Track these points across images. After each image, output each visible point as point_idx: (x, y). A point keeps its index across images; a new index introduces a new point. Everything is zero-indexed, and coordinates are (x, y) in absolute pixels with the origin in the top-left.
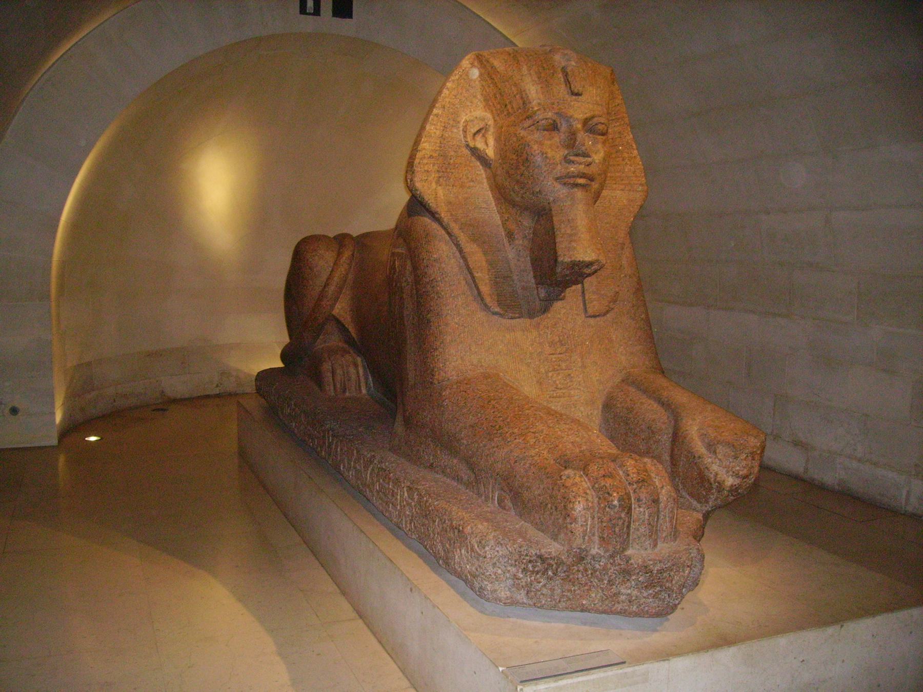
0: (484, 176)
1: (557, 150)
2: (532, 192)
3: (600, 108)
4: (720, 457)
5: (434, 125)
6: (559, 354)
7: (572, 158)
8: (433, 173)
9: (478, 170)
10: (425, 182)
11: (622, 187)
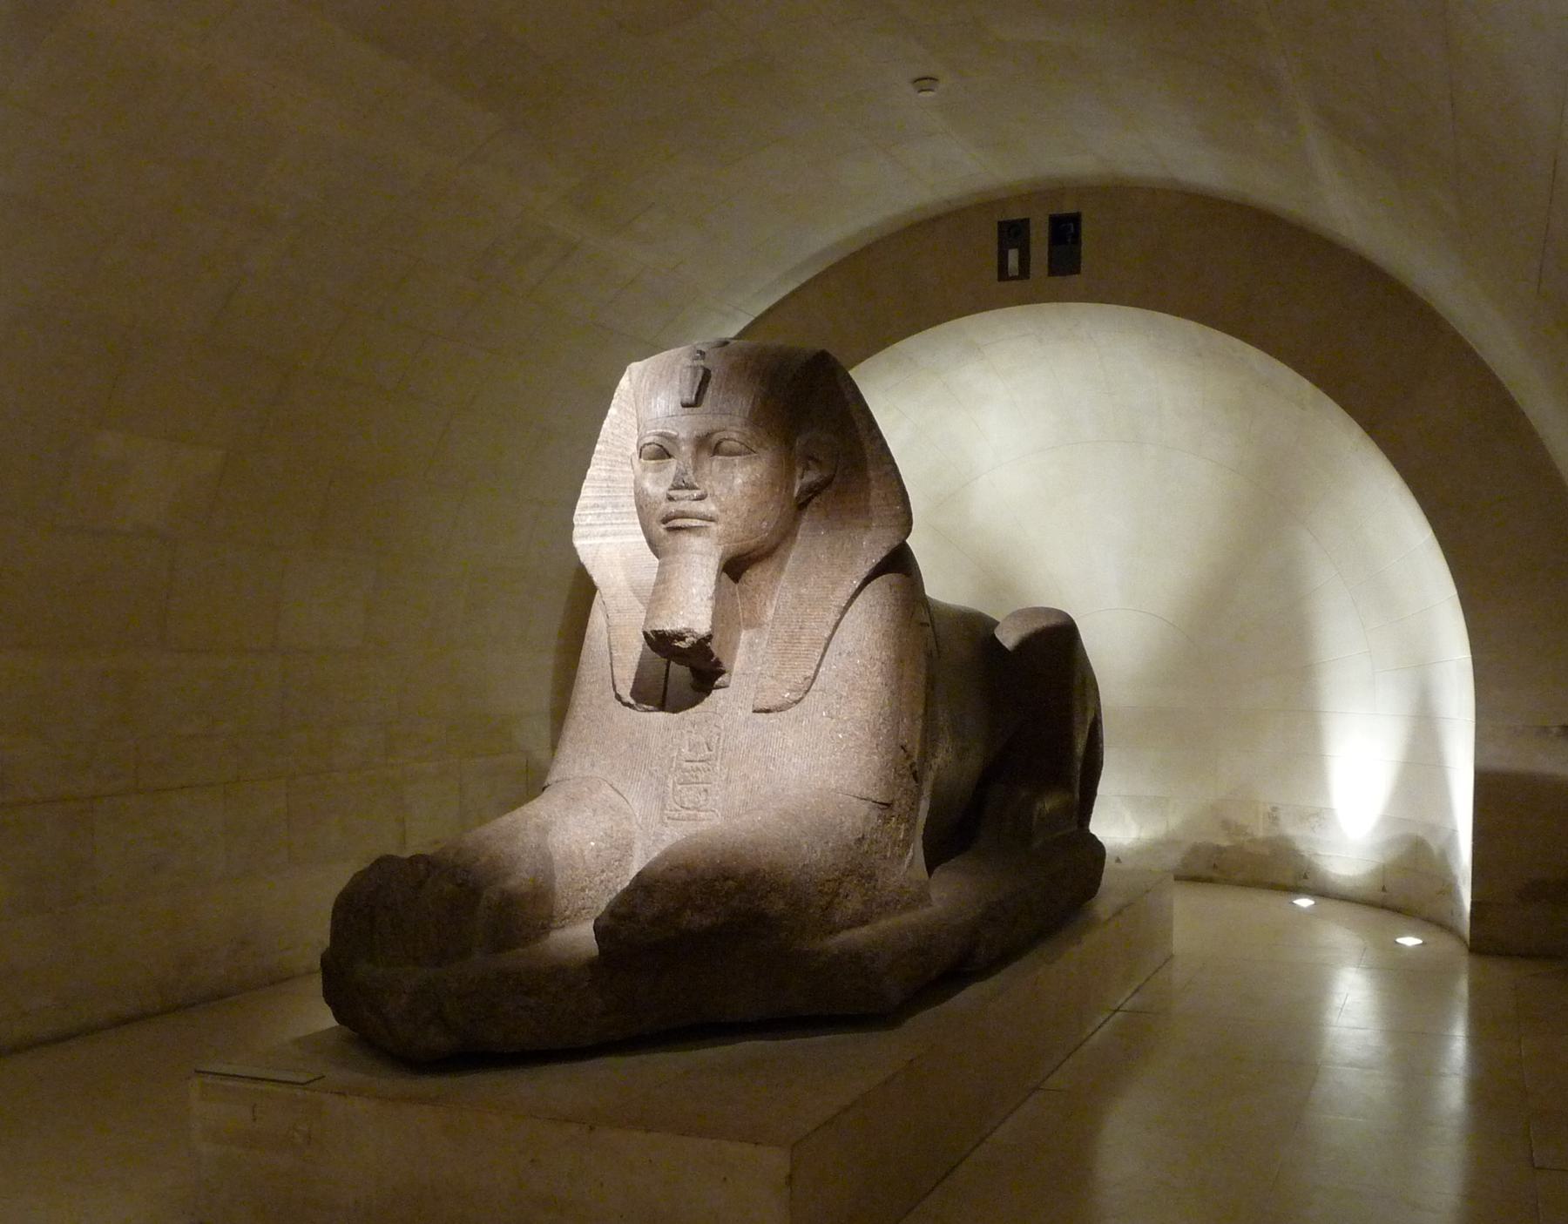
5: (597, 464)
7: (673, 493)
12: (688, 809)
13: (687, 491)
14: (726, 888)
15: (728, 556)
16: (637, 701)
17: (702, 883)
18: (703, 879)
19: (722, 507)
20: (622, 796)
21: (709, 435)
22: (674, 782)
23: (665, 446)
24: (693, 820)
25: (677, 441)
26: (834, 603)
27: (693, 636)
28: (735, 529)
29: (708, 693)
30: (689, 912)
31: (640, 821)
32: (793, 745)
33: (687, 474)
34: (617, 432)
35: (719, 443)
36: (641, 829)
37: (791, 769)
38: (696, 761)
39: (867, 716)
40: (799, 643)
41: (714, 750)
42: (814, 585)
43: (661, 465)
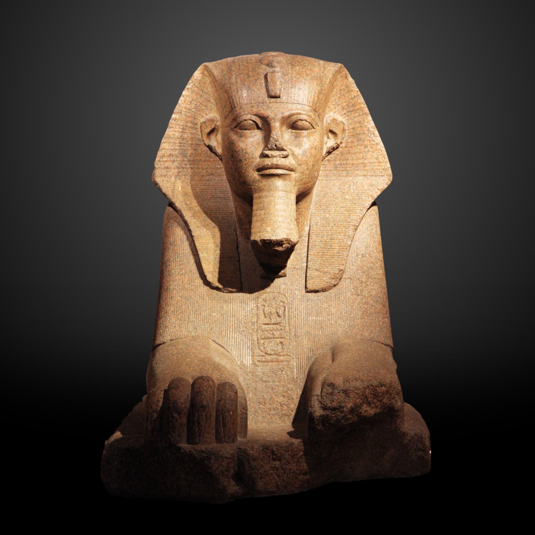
0: (223, 169)
1: (256, 146)
3: (299, 106)
5: (173, 128)
6: (273, 324)
7: (267, 152)
8: (173, 169)
9: (218, 165)
10: (165, 177)
11: (365, 173)
12: (270, 355)
13: (278, 152)
14: (382, 391)
15: (298, 193)
16: (225, 286)
17: (372, 388)
18: (372, 386)
19: (299, 163)
20: (224, 348)
21: (290, 116)
22: (257, 337)
23: (258, 122)
24: (276, 361)
25: (268, 120)
26: (351, 224)
27: (289, 244)
28: (305, 177)
29: (272, 281)
30: (365, 406)
31: (239, 363)
32: (336, 313)
33: (278, 141)
34: (188, 106)
35: (296, 121)
36: (241, 368)
37: (338, 327)
38: (270, 324)
39: (379, 294)
40: (332, 248)
41: (283, 316)
42: (335, 211)
43: (253, 134)
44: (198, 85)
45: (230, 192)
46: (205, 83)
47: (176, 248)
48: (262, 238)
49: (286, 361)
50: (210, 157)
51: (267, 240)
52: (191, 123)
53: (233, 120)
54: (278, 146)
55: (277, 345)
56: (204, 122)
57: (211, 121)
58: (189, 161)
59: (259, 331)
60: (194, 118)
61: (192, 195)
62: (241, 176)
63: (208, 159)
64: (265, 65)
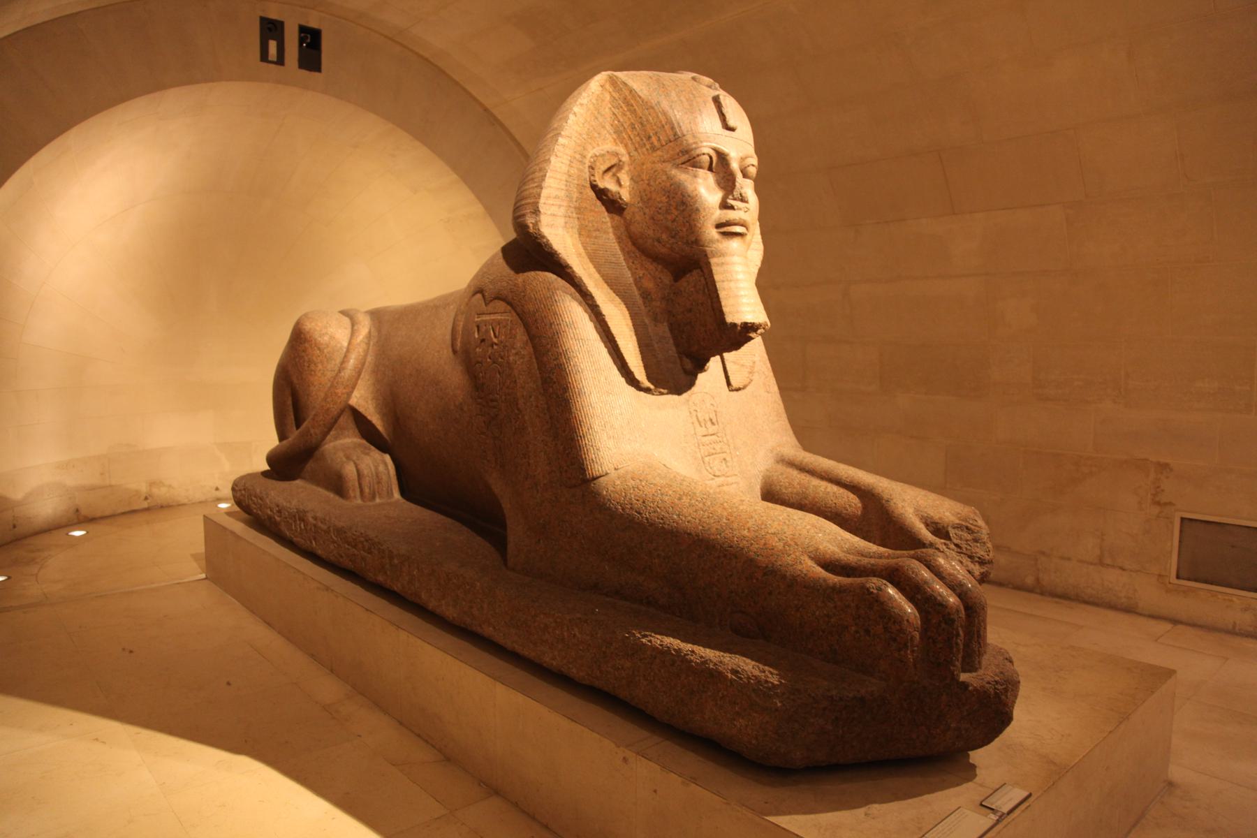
0: (609, 224)
2: (685, 241)
4: (956, 541)
12: (718, 476)
16: (656, 386)
25: (728, 158)
34: (579, 129)
35: (748, 166)
44: (595, 102)
45: (621, 256)
46: (603, 100)
47: (578, 332)
48: (743, 321)
49: (735, 483)
50: (595, 205)
51: (751, 323)
52: (580, 154)
53: (681, 151)
54: (743, 195)
55: (722, 462)
56: (602, 155)
57: (613, 155)
58: (575, 208)
59: (701, 447)
60: (584, 147)
61: (586, 257)
62: (693, 233)
63: (593, 208)
64: (704, 85)
